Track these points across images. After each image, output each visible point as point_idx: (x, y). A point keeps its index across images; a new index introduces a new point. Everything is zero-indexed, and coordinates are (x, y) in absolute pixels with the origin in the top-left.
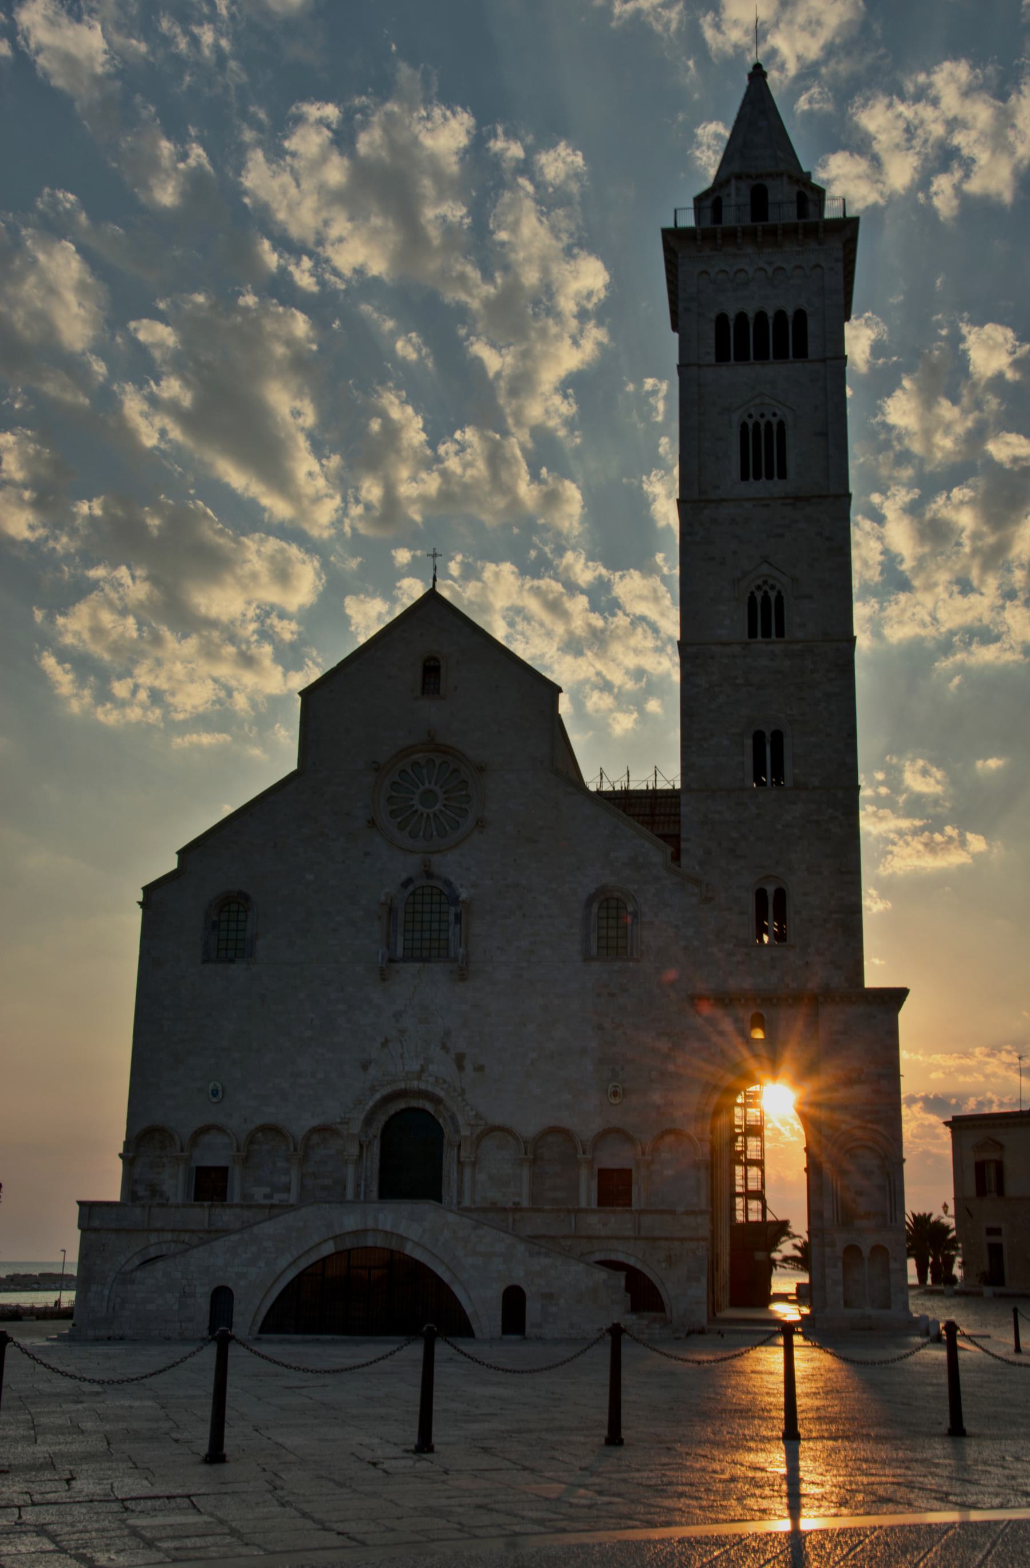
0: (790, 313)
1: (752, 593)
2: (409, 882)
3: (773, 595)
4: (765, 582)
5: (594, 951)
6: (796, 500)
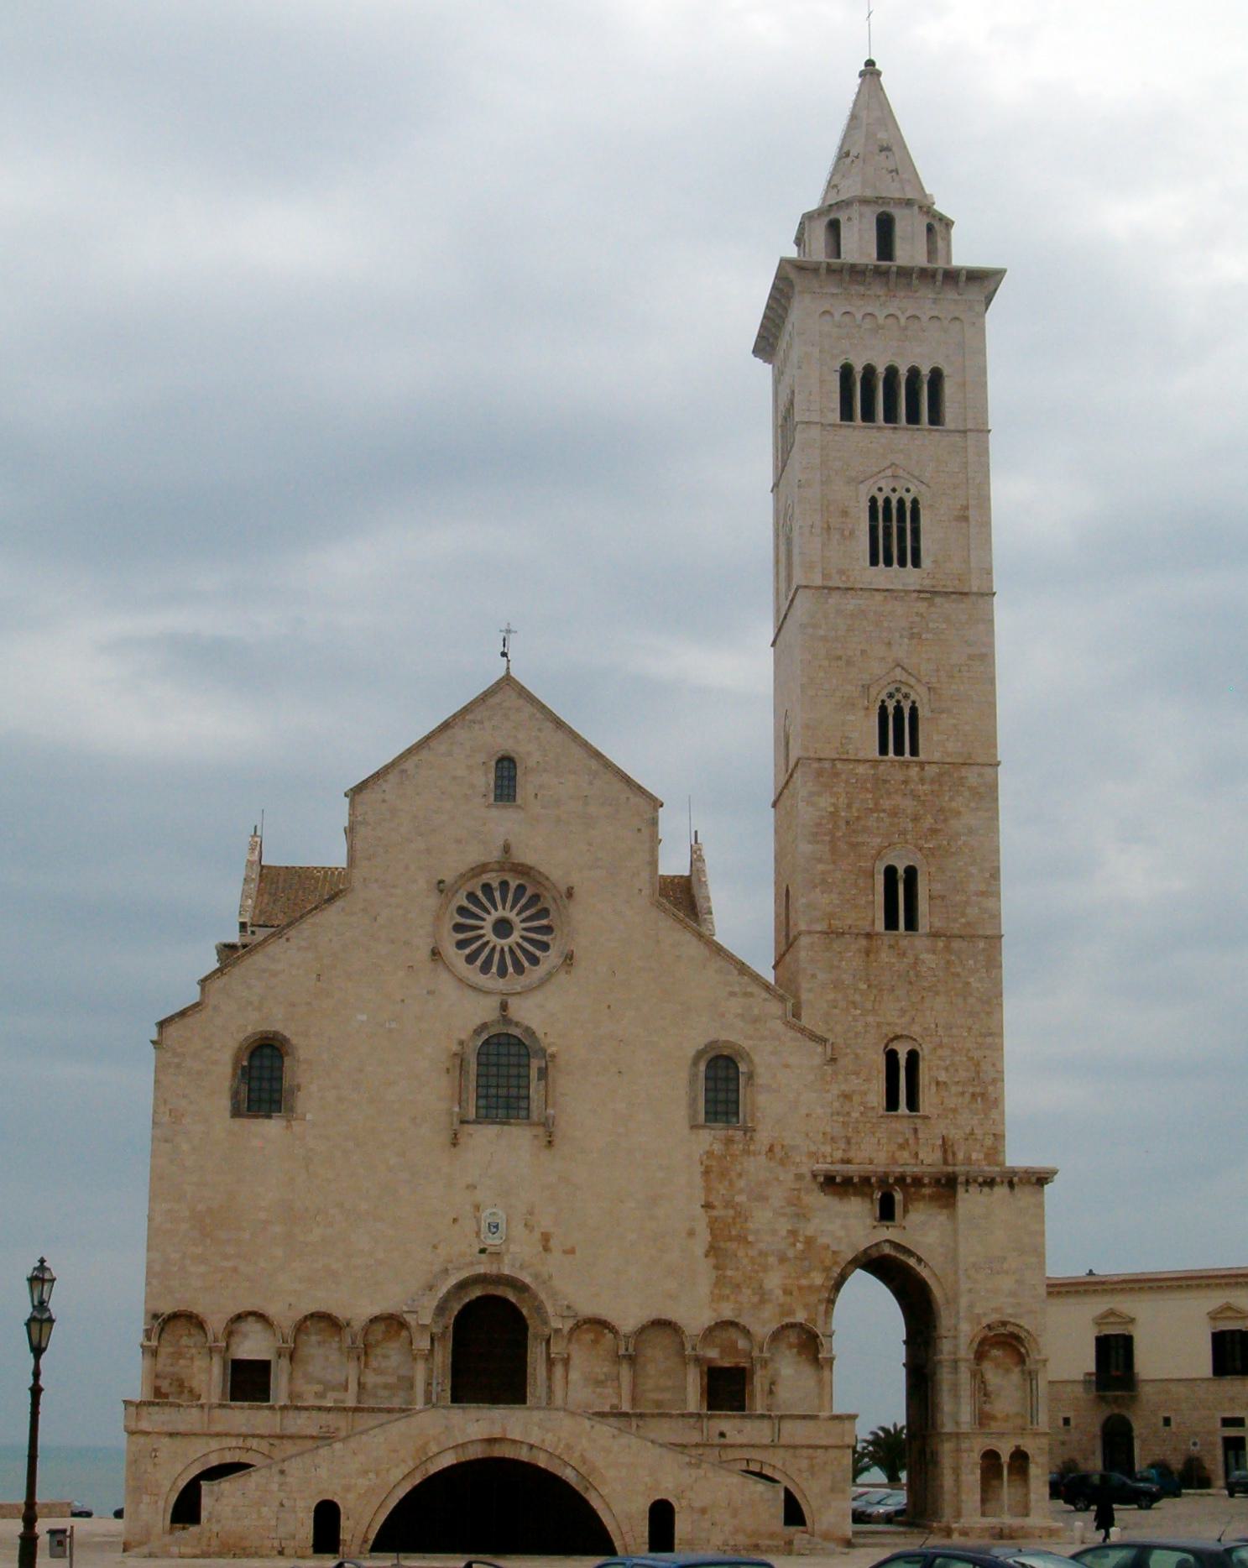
1: (883, 701)
2: (484, 1026)
4: (898, 690)
5: (701, 1117)
6: (930, 594)
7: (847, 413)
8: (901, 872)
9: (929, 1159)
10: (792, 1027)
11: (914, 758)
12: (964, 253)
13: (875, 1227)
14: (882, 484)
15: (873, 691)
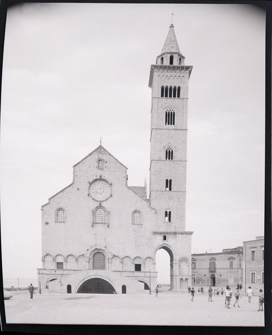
0: (177, 87)
1: (167, 150)
3: (171, 150)
4: (169, 148)
7: (162, 96)
8: (169, 180)
9: (173, 230)
10: (149, 207)
11: (172, 160)
12: (186, 63)
13: (163, 241)
14: (168, 109)
15: (165, 148)
